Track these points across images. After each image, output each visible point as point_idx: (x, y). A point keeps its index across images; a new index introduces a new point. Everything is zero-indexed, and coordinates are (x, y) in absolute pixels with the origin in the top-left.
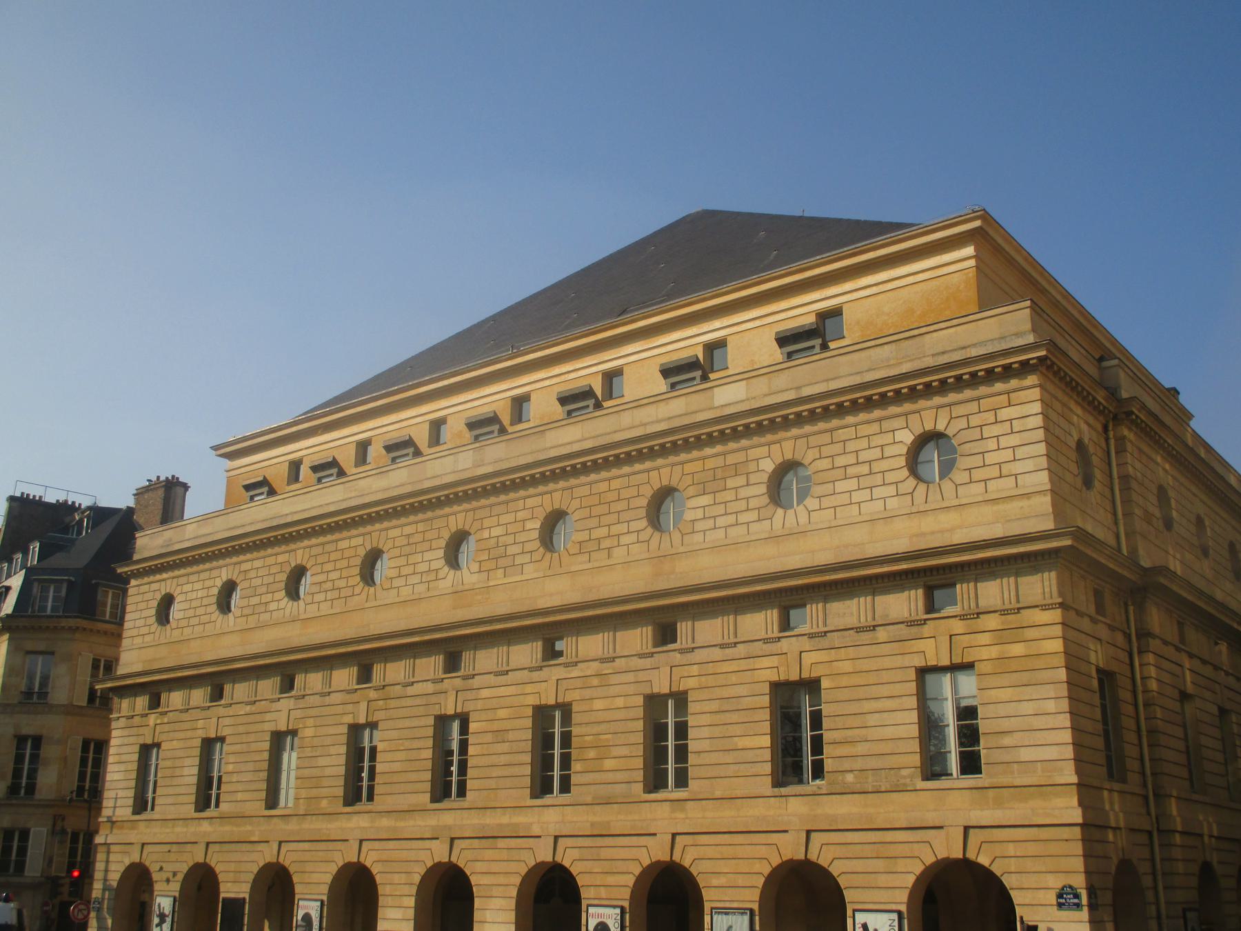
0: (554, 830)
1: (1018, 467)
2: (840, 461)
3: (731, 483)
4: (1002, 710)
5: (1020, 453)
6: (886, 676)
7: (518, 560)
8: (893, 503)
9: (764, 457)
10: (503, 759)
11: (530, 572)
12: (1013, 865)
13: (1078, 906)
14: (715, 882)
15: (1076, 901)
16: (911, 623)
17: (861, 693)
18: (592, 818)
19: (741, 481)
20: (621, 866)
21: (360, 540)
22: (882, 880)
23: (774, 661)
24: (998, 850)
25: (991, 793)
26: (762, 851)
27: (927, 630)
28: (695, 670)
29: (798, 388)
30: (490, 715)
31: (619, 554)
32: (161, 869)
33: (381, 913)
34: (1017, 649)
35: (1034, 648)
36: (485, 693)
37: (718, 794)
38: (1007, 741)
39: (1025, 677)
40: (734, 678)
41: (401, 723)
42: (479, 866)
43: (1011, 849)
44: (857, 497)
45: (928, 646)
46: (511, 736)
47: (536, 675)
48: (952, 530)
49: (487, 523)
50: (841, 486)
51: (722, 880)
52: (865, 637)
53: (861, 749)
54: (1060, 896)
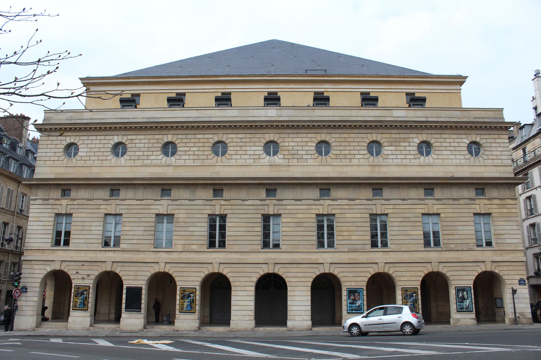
0: (329, 261)
1: (503, 157)
2: (444, 144)
3: (402, 144)
4: (501, 228)
5: (503, 153)
6: (463, 215)
7: (304, 157)
9: (417, 138)
10: (301, 234)
11: (310, 162)
12: (505, 273)
13: (525, 284)
14: (402, 279)
16: (471, 199)
17: (455, 219)
18: (350, 257)
19: (407, 144)
20: (363, 274)
21: (211, 136)
22: (465, 278)
23: (423, 206)
24: (501, 268)
25: (498, 252)
26: (421, 269)
27: (477, 202)
28: (391, 207)
29: (427, 117)
30: (293, 216)
31: (354, 162)
32: (77, 273)
33: (233, 293)
34: (505, 210)
35: (510, 211)
36: (289, 207)
37: (403, 250)
38: (502, 237)
39: (507, 219)
40: (407, 211)
41: (241, 216)
42: (290, 275)
43: (505, 268)
44: (450, 157)
45: (477, 207)
46: (305, 225)
47: (317, 203)
48: (483, 172)
49: (286, 140)
50: (444, 153)
51: (406, 279)
52: (456, 202)
54: (519, 281)
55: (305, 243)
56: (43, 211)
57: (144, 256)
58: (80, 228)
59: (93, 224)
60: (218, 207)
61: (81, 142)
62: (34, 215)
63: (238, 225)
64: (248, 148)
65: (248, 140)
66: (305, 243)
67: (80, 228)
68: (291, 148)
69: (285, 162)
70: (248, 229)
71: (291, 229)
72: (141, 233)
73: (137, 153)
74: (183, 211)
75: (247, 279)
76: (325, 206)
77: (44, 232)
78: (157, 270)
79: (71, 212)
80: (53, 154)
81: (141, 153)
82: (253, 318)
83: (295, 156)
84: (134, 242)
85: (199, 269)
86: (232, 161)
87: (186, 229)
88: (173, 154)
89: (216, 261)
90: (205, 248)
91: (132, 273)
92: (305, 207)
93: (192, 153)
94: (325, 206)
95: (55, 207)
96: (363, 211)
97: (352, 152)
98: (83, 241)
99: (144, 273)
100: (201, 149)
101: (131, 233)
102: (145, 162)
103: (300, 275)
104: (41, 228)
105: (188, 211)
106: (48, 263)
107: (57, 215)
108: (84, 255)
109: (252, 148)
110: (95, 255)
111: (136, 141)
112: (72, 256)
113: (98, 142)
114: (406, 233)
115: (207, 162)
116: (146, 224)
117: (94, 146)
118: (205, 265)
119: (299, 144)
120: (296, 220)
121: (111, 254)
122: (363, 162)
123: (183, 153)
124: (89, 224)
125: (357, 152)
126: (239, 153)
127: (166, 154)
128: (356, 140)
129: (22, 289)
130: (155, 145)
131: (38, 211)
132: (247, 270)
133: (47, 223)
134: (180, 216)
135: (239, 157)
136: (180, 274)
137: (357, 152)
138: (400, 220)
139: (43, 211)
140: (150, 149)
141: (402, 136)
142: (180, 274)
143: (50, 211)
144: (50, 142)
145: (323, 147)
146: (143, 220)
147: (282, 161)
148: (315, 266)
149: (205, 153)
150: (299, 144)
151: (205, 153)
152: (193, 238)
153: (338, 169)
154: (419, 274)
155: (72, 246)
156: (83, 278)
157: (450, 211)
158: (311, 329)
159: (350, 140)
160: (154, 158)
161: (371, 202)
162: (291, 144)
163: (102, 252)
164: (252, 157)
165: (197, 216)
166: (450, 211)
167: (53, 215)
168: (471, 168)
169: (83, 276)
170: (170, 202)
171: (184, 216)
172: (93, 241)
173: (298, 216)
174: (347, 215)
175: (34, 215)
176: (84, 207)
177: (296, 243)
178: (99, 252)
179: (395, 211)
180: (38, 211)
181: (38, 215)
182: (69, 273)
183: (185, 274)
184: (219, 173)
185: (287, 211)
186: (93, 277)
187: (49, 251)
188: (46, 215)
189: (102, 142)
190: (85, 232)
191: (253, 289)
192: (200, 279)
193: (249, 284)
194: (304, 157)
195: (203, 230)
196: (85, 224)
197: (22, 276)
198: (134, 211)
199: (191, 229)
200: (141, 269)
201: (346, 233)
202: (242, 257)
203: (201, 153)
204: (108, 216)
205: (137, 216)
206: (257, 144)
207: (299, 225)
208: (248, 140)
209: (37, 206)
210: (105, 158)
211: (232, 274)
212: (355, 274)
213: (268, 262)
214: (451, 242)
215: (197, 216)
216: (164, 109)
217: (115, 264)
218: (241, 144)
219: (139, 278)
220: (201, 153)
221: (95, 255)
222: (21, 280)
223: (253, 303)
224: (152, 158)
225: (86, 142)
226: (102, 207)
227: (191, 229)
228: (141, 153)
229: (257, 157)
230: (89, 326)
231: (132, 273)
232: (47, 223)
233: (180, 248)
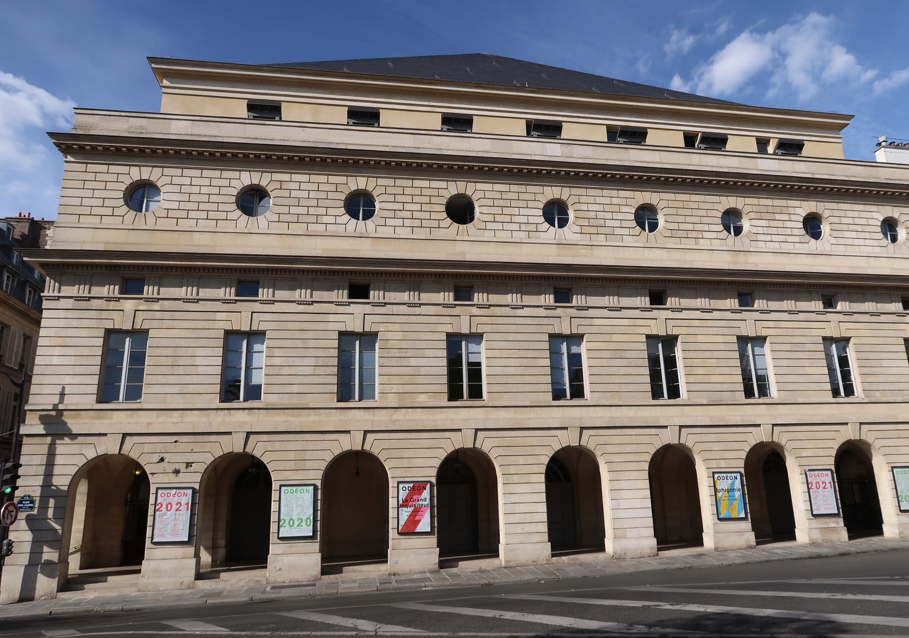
7: (617, 231)
8: (877, 250)
10: (622, 371)
11: (628, 241)
17: (877, 348)
19: (786, 217)
28: (771, 324)
30: (606, 337)
31: (703, 244)
32: (162, 460)
41: (511, 337)
51: (809, 453)
53: (881, 378)
55: (631, 388)
56: (74, 323)
57: (317, 418)
58: (169, 361)
59: (199, 352)
60: (465, 320)
61: (167, 180)
62: (52, 332)
63: (505, 354)
64: (516, 211)
65: (515, 196)
66: (631, 388)
67: (169, 361)
68: (592, 215)
69: (585, 239)
70: (525, 362)
71: (604, 362)
72: (309, 370)
73: (294, 210)
74: (397, 327)
75: (530, 460)
76: (659, 322)
77: (78, 370)
78: (347, 447)
79: (144, 327)
80: (99, 202)
81: (304, 210)
82: (546, 537)
83: (601, 230)
84: (295, 389)
85: (434, 443)
86: (487, 233)
87: (404, 362)
88: (369, 215)
89: (464, 424)
90: (444, 400)
91: (292, 456)
92: (626, 322)
93: (409, 215)
94: (659, 322)
95: (105, 314)
96: (726, 331)
97: (698, 227)
98: (176, 389)
99: (319, 455)
100: (425, 207)
101: (285, 371)
102: (311, 227)
103: (628, 449)
104: (71, 360)
105: (406, 327)
108: (178, 420)
109: (523, 211)
111: (291, 186)
113: (206, 182)
114: (801, 371)
115: (438, 234)
116: (320, 353)
117: (196, 190)
118: (447, 434)
119: (607, 208)
120: (612, 346)
122: (717, 244)
123: (391, 214)
124: (190, 352)
125: (706, 228)
126: (498, 218)
127: (354, 214)
128: (702, 206)
129: (20, 502)
130: (331, 195)
131: (62, 323)
132: (529, 441)
133: (86, 351)
134: (390, 336)
135: (498, 226)
136: (395, 454)
137: (706, 228)
138: (788, 347)
139: (74, 323)
140: (321, 203)
141: (777, 202)
142: (395, 454)
143: (93, 323)
144: (91, 176)
145: (646, 217)
146: (312, 343)
147: (578, 236)
148: (653, 431)
149: (434, 216)
150: (607, 208)
151: (434, 216)
152: (420, 380)
153: (677, 255)
154: (830, 444)
155: (145, 401)
156: (177, 472)
157: (868, 333)
158: (658, 555)
159: (692, 205)
160: (331, 220)
161: (737, 316)
162: (591, 207)
163: (222, 412)
164: (523, 227)
165: (424, 336)
166: (868, 333)
167: (101, 333)
168: (891, 261)
169: (177, 466)
170: (368, 309)
171: (399, 336)
173: (616, 338)
174: (700, 339)
175: (52, 332)
176: (177, 315)
177: (615, 388)
179: (779, 332)
180: (62, 323)
183: (406, 453)
184: (463, 254)
185: (594, 329)
186: (202, 468)
188: (84, 333)
189: (215, 182)
190: (180, 370)
191: (542, 478)
192: (437, 463)
193: (536, 469)
194: (617, 231)
195: (437, 363)
196: (180, 352)
197: (21, 471)
198: (291, 326)
199: (413, 362)
200: (311, 446)
201: (701, 371)
202: (519, 416)
203: (427, 216)
204: (231, 337)
205: (297, 335)
206: (531, 204)
207: (618, 354)
208: (515, 196)
209: (62, 314)
210: (223, 215)
211: (501, 451)
212: (723, 446)
213: (565, 424)
214: (875, 387)
215: (424, 336)
216: (344, 127)
217: (370, 437)
218: (502, 203)
219: (308, 465)
220: (427, 216)
221: (205, 420)
222: (19, 482)
223: (543, 508)
224: (326, 219)
225: (176, 180)
226: (219, 316)
227: (413, 362)
228: (304, 210)
229: (533, 228)
231: (292, 456)
232: (86, 351)
233: (393, 401)
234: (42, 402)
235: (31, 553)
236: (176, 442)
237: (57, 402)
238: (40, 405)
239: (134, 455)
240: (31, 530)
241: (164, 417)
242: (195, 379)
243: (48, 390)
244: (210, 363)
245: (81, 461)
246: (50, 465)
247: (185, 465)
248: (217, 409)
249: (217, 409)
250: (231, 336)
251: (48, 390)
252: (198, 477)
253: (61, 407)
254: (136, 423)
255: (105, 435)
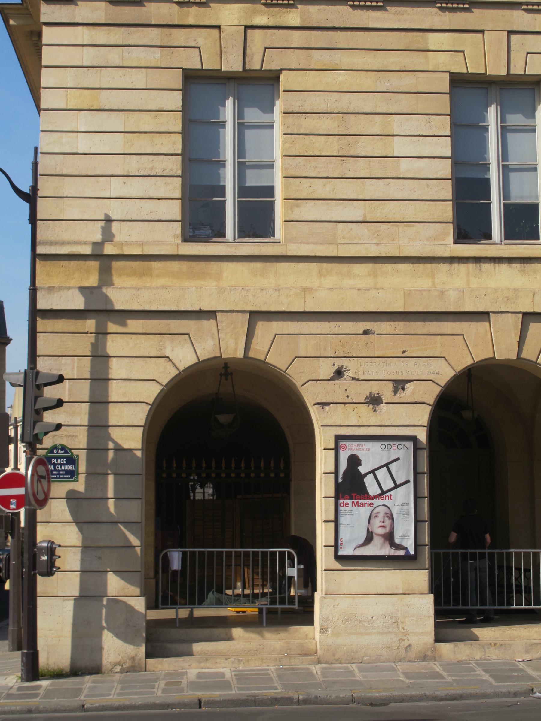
15: (70, 467)
32: (339, 373)
56: (114, 56)
58: (332, 146)
59: (398, 124)
62: (69, 78)
67: (332, 146)
77: (133, 165)
79: (271, 65)
98: (355, 212)
104: (117, 143)
106: (174, 325)
107: (191, 78)
108: (369, 282)
110: (424, 283)
112: (305, 290)
121: (505, 277)
124: (376, 125)
131: (89, 56)
133: (147, 122)
139: (114, 56)
156: (375, 401)
163: (462, 268)
167: (175, 80)
169: (375, 388)
172: (410, 211)
175: (69, 78)
178: (444, 267)
181: (92, 79)
182: (297, 375)
186: (431, 393)
187: (175, 265)
188: (138, 79)
190: (360, 167)
196: (357, 125)
221: (424, 283)
226: (435, 41)
230: (431, 638)
232: (147, 122)
234: (66, 236)
235: (83, 571)
236: (366, 333)
237: (98, 238)
238: (63, 243)
239: (277, 360)
240: (79, 522)
241: (334, 275)
242: (395, 189)
243: (73, 210)
244: (423, 151)
245: (166, 374)
246: (100, 379)
247: (391, 385)
248: (452, 260)
249: (452, 260)
250: (469, 89)
251: (73, 210)
252: (423, 415)
253: (109, 249)
254: (277, 289)
255: (211, 314)
